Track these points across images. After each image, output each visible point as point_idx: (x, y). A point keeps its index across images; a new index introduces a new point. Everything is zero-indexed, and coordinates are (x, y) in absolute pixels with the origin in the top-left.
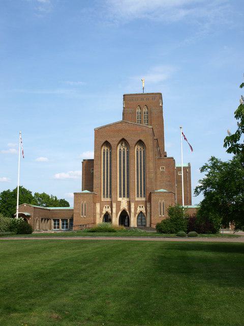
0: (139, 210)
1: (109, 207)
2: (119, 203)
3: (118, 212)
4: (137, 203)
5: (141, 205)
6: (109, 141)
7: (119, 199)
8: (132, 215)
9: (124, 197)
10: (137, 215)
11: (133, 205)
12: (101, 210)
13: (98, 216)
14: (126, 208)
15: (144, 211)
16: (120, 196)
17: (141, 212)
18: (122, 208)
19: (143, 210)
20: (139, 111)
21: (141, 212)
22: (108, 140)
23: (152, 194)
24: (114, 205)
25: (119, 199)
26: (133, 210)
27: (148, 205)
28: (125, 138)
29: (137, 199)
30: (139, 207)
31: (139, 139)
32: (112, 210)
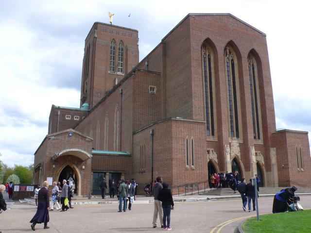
6: (212, 39)
27: (273, 152)
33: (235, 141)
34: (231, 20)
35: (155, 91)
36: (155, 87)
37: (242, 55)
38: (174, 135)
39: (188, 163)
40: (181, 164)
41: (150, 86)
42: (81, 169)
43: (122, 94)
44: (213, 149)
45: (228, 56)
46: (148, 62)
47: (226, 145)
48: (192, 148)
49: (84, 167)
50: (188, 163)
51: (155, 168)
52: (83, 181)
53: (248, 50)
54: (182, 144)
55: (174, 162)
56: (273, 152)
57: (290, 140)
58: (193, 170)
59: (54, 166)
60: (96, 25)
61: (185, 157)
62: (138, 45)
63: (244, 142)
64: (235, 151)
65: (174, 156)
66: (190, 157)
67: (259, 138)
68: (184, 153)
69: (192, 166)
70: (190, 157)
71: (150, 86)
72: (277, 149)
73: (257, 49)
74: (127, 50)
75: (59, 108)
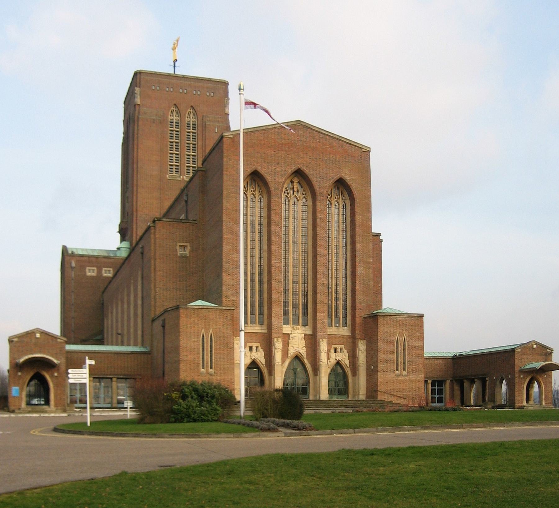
2: (287, 338)
4: (331, 339)
5: (339, 347)
9: (296, 323)
11: (323, 346)
14: (303, 352)
16: (287, 323)
17: (338, 363)
18: (292, 352)
19: (344, 357)
20: (175, 118)
21: (338, 363)
22: (259, 169)
24: (278, 344)
25: (286, 329)
26: (323, 356)
28: (304, 169)
29: (333, 331)
31: (337, 177)
33: (296, 332)
36: (188, 244)
37: (318, 190)
38: (182, 329)
40: (192, 368)
41: (179, 244)
42: (52, 376)
43: (142, 253)
44: (258, 345)
45: (295, 194)
46: (187, 195)
47: (275, 340)
48: (211, 346)
49: (56, 374)
51: (166, 373)
52: (56, 390)
53: (329, 183)
54: (194, 341)
55: (182, 366)
56: (362, 347)
57: (383, 328)
58: (211, 375)
59: (20, 374)
60: (137, 75)
61: (198, 358)
62: (227, 115)
63: (313, 332)
64: (296, 346)
65: (182, 357)
66: (207, 358)
68: (198, 353)
70: (207, 358)
72: (367, 342)
73: (348, 176)
74: (204, 127)
75: (73, 255)
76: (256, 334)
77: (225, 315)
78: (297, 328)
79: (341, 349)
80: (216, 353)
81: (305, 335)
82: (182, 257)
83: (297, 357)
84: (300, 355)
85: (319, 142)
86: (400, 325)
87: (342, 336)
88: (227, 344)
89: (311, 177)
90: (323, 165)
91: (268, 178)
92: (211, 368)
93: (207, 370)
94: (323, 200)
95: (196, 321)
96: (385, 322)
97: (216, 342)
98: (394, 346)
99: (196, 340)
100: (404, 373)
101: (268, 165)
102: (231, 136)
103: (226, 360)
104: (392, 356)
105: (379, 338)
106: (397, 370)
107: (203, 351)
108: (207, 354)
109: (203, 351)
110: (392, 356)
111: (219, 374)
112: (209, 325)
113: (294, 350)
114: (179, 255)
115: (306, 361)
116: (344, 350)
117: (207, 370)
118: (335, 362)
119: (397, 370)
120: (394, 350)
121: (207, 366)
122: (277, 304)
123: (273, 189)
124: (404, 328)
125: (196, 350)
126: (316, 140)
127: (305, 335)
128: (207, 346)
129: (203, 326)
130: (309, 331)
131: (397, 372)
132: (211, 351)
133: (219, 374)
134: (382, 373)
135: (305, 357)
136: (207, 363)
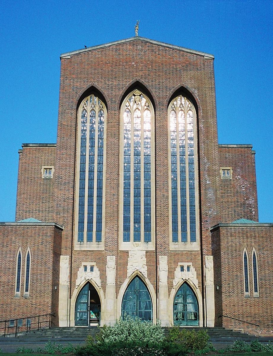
0: (179, 277)
1: (96, 269)
3: (121, 283)
5: (185, 265)
7: (124, 246)
8: (163, 289)
9: (137, 238)
10: (173, 292)
11: (163, 262)
12: (72, 276)
13: (63, 294)
14: (144, 271)
15: (194, 281)
16: (127, 238)
23: (223, 231)
24: (111, 262)
25: (124, 246)
26: (163, 275)
28: (143, 81)
30: (178, 269)
32: (103, 276)
34: (139, 47)
35: (52, 175)
36: (52, 167)
39: (18, 288)
40: (6, 291)
41: (43, 167)
44: (94, 264)
50: (18, 288)
64: (135, 265)
66: (23, 279)
67: (193, 239)
68: (13, 274)
69: (25, 293)
70: (23, 279)
71: (43, 167)
76: (92, 253)
77: (45, 232)
78: (136, 244)
79: (188, 267)
80: (33, 274)
81: (147, 252)
82: (46, 179)
83: (138, 277)
84: (141, 275)
85: (159, 54)
86: (247, 238)
87: (189, 253)
88: (45, 263)
89: (149, 88)
90: (162, 75)
91: (105, 93)
92: (27, 290)
93: (22, 293)
94: (163, 109)
95: (13, 238)
96: (229, 234)
97: (34, 261)
98: (241, 262)
99: (12, 259)
100: (256, 294)
101: (105, 81)
102: (69, 57)
103: (43, 281)
104: (239, 274)
105: (222, 252)
106: (247, 291)
107: (19, 271)
108: (23, 274)
109: (19, 271)
110: (239, 274)
111: (34, 296)
112: (27, 243)
113: (134, 268)
114: (43, 178)
115: (147, 281)
116: (192, 268)
117: (22, 293)
118: (182, 282)
119: (247, 291)
120: (241, 266)
121: (22, 288)
122: (112, 218)
123: (110, 102)
124: (253, 240)
125: (11, 270)
126: (155, 53)
127: (147, 252)
128: (23, 265)
129: (20, 244)
130: (151, 246)
131: (246, 293)
132: (28, 271)
133: (34, 296)
134: (228, 294)
135: (146, 277)
136: (22, 285)
